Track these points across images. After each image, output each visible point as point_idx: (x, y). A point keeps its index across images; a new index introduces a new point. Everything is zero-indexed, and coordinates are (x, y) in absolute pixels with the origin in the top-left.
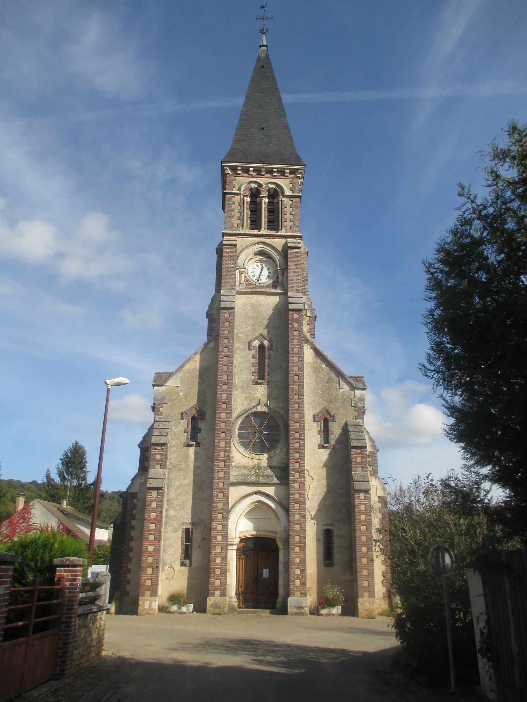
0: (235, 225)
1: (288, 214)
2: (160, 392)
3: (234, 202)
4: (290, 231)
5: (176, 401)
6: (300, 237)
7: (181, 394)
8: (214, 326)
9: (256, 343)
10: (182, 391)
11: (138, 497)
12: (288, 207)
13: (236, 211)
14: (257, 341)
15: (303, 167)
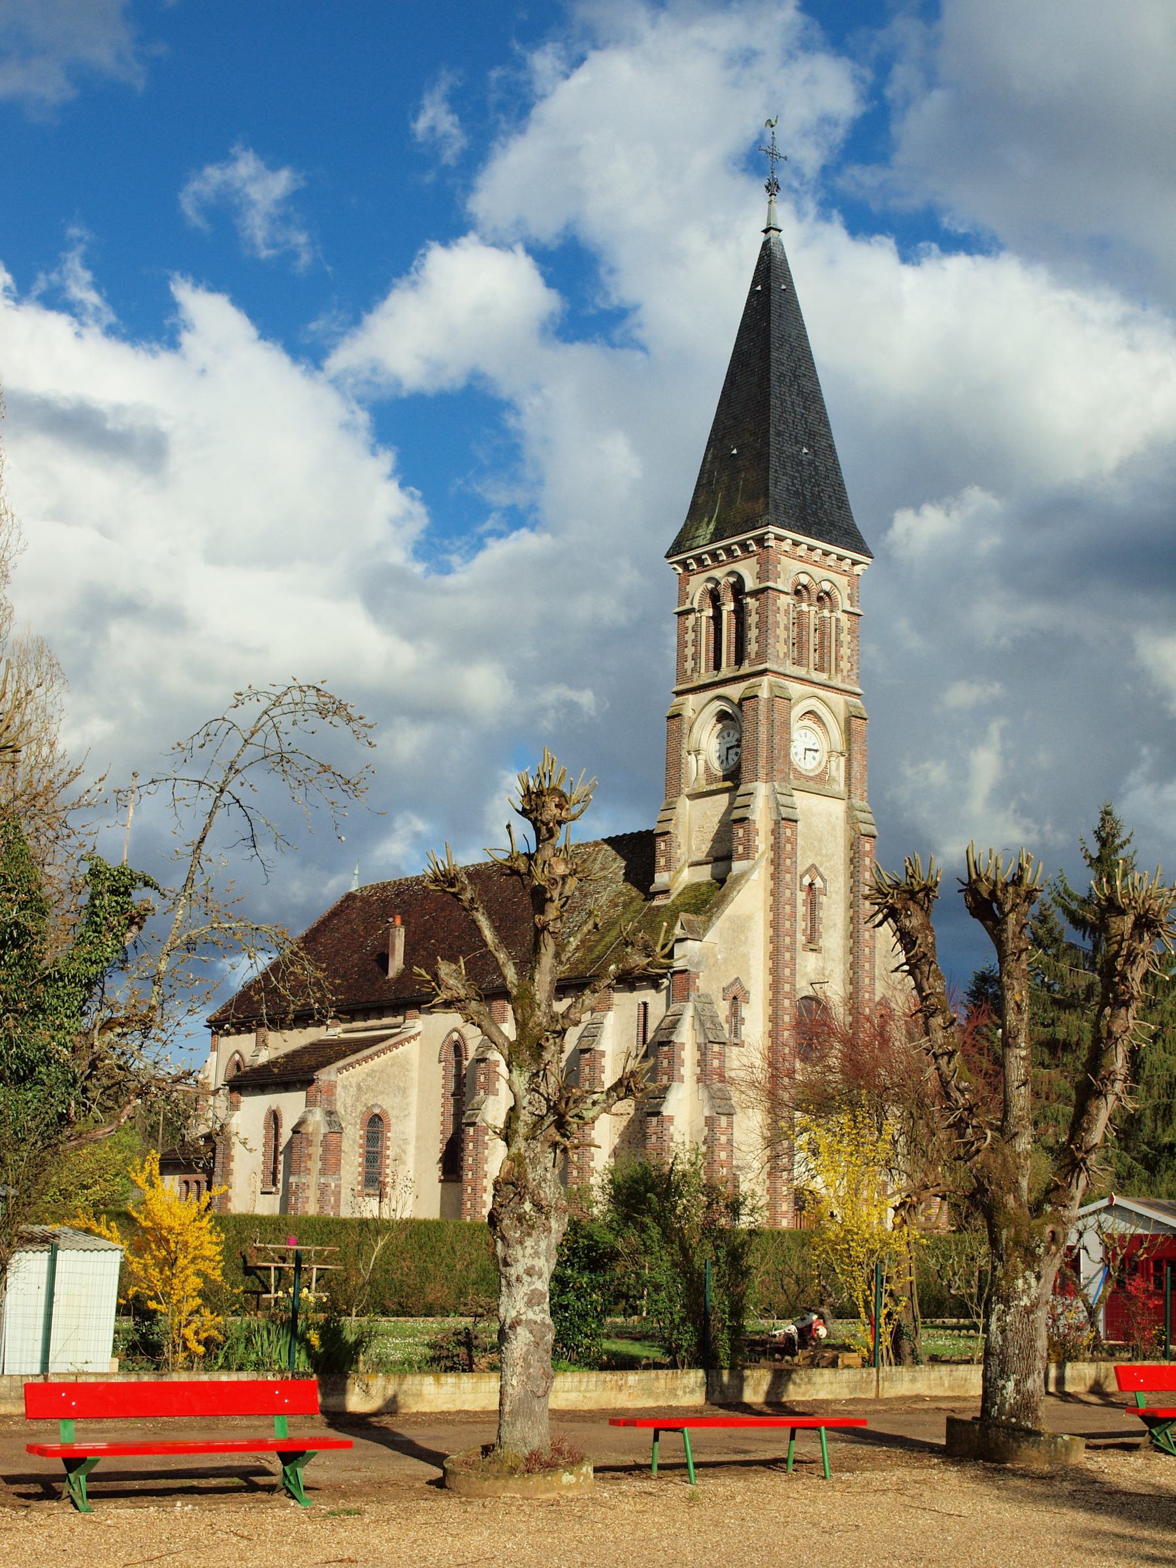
0: (781, 655)
1: (845, 645)
2: (696, 950)
3: (779, 609)
4: (847, 680)
5: (714, 969)
6: (859, 695)
7: (719, 957)
8: (757, 843)
9: (807, 880)
10: (720, 952)
11: (675, 1123)
12: (846, 631)
13: (782, 626)
14: (807, 876)
15: (868, 560)
